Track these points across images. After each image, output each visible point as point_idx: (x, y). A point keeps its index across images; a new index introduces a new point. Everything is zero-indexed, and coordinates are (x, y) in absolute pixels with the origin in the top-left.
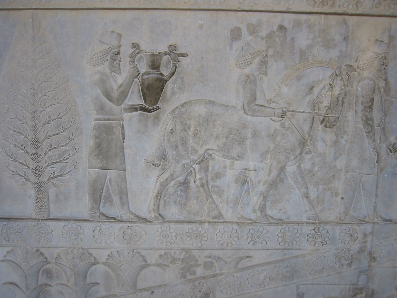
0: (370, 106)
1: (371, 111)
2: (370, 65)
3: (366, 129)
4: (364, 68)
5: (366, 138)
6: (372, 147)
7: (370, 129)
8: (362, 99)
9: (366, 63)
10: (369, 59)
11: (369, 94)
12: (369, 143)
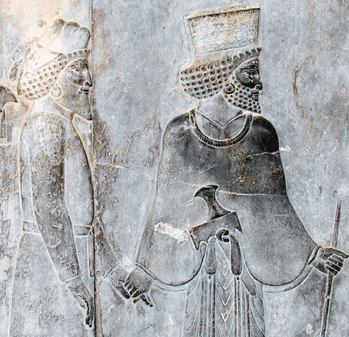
0: (54, 184)
1: (56, 198)
2: (45, 84)
3: (50, 243)
4: (32, 91)
5: (52, 263)
6: (69, 285)
7: (59, 243)
8: (34, 169)
9: (35, 80)
10: (42, 69)
11: (47, 157)
12: (60, 276)
